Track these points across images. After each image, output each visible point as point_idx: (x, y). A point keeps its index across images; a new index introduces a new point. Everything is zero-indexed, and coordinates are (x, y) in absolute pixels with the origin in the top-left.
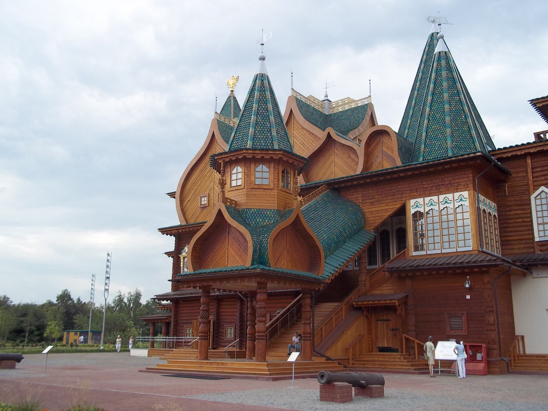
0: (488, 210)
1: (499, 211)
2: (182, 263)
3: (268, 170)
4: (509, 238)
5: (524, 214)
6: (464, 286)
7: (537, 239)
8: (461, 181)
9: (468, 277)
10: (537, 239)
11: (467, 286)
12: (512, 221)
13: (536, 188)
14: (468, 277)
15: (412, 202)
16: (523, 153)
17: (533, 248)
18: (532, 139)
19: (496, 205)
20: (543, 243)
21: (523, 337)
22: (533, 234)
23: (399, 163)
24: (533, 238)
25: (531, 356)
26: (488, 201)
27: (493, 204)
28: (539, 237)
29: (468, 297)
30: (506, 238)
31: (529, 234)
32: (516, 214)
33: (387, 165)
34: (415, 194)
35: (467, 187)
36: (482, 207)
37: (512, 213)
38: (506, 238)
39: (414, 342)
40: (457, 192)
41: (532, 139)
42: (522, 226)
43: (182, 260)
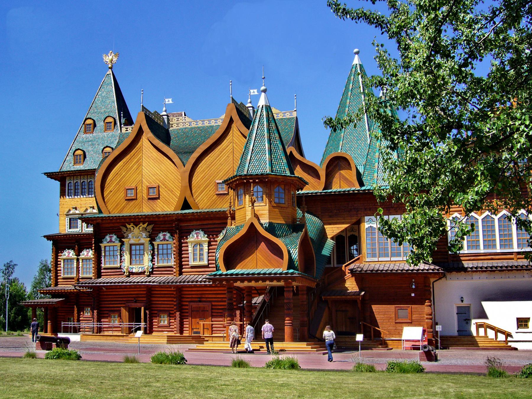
2: (103, 252)
9: (413, 280)
11: (414, 287)
15: (367, 218)
29: (413, 295)
34: (369, 212)
39: (370, 328)
43: (103, 249)
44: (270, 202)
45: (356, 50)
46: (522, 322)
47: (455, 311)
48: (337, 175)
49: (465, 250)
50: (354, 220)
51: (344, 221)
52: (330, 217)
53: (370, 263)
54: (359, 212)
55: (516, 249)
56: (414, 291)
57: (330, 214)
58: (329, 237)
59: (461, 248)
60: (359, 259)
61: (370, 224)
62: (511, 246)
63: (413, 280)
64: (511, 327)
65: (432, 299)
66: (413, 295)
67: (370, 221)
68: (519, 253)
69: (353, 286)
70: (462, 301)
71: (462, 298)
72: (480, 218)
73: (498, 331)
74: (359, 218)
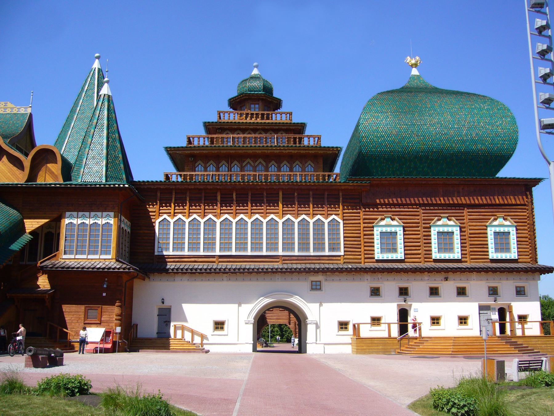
7: (156, 254)
9: (106, 279)
10: (156, 254)
11: (105, 286)
13: (160, 214)
14: (106, 279)
18: (163, 179)
21: (137, 325)
23: (61, 182)
24: (154, 252)
25: (140, 339)
27: (129, 223)
29: (104, 294)
33: (50, 180)
37: (141, 232)
41: (163, 179)
45: (97, 55)
46: (219, 325)
47: (156, 312)
49: (171, 252)
53: (66, 260)
55: (218, 253)
56: (106, 290)
59: (167, 249)
60: (55, 255)
61: (71, 221)
62: (213, 249)
64: (208, 329)
65: (123, 299)
67: (71, 217)
68: (221, 257)
69: (45, 284)
70: (163, 303)
71: (163, 299)
73: (193, 332)
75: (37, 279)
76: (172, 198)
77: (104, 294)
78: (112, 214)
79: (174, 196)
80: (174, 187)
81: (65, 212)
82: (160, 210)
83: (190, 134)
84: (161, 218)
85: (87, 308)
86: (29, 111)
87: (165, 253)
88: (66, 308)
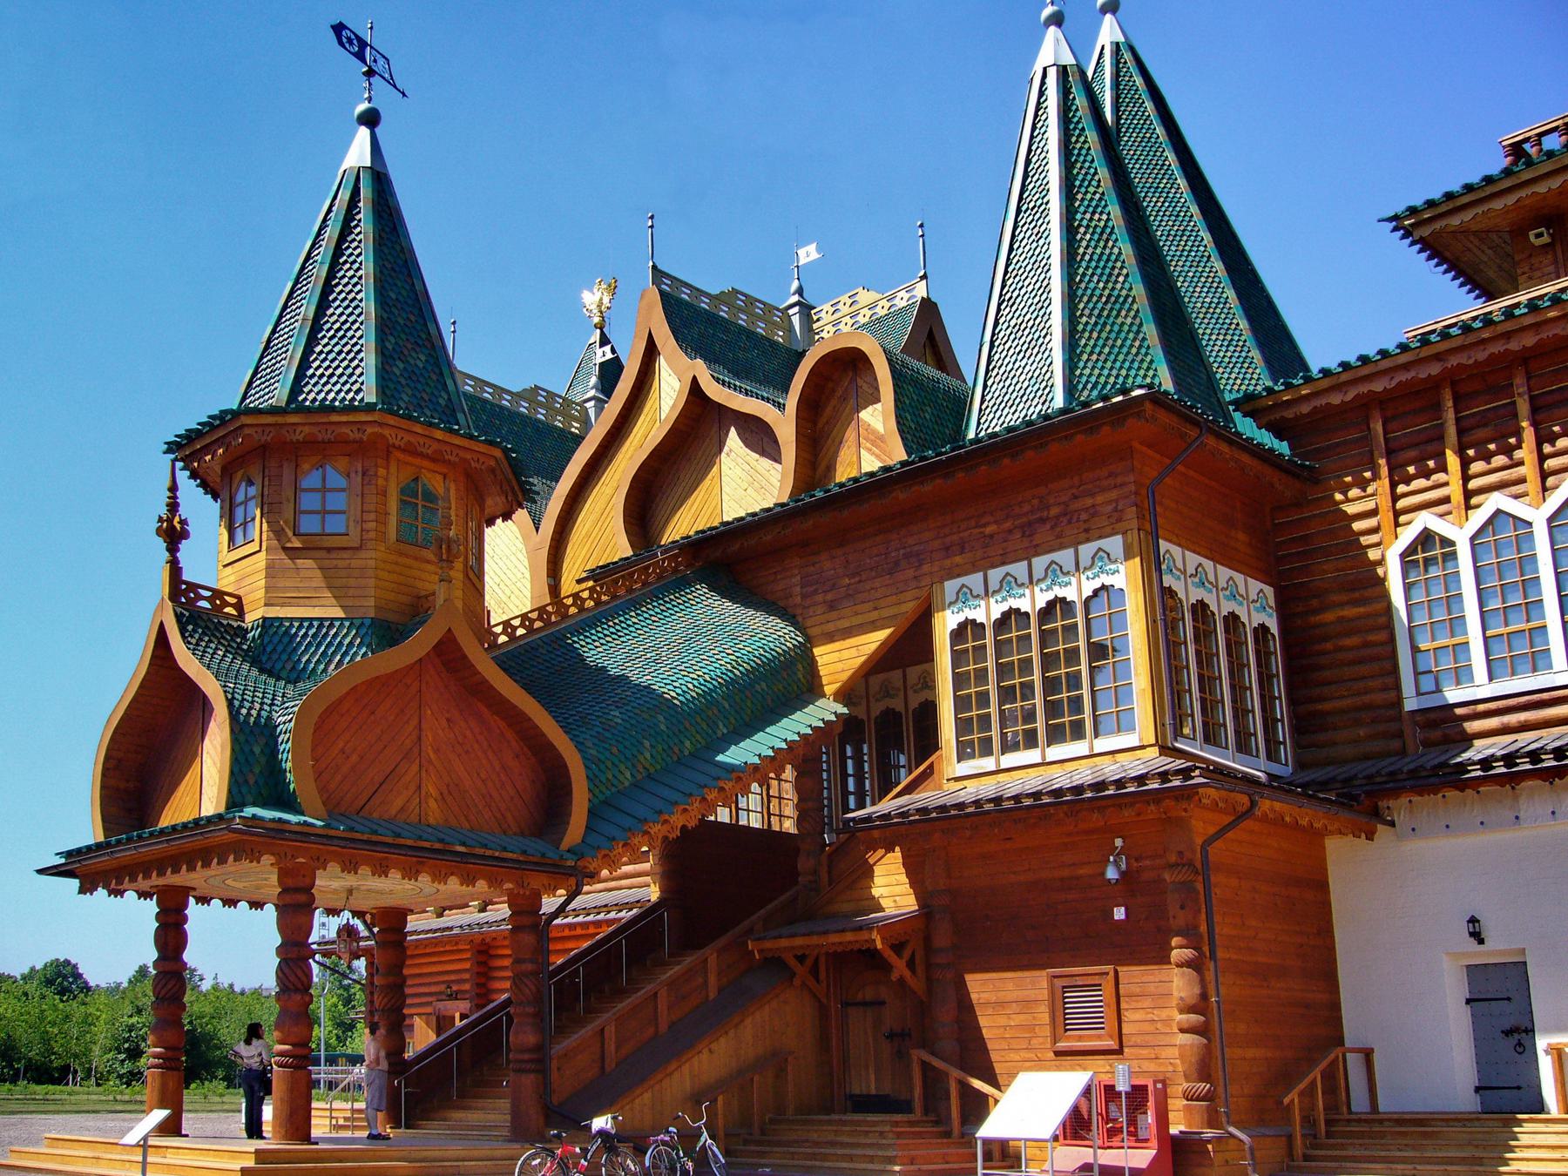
0: (1221, 607)
1: (1283, 608)
3: (343, 483)
4: (1327, 706)
5: (1368, 615)
6: (1103, 874)
7: (1410, 704)
8: (1099, 499)
10: (1410, 704)
11: (1111, 874)
12: (1329, 646)
16: (1350, 396)
17: (1399, 735)
19: (1269, 591)
20: (1432, 716)
22: (1397, 687)
26: (1224, 573)
27: (1255, 586)
28: (1419, 694)
30: (1311, 707)
31: (1385, 689)
32: (1341, 619)
35: (1119, 520)
36: (1190, 594)
37: (1329, 616)
38: (1311, 707)
40: (1088, 540)
42: (1360, 661)
44: (278, 533)
47: (1453, 991)
48: (850, 434)
49: (1481, 687)
50: (909, 607)
51: (875, 615)
52: (832, 606)
53: (965, 783)
54: (926, 568)
57: (829, 597)
58: (829, 690)
59: (1462, 675)
60: (931, 766)
63: (1118, 842)
65: (1203, 928)
66: (1119, 913)
69: (898, 890)
71: (1473, 920)
72: (1538, 515)
74: (924, 593)
75: (868, 872)
76: (1441, 427)
77: (1119, 913)
78: (1114, 544)
79: (1450, 415)
80: (1435, 369)
81: (942, 581)
82: (1395, 498)
83: (1517, 135)
84: (1407, 535)
85: (1059, 983)
86: (921, 291)
87: (1453, 695)
88: (982, 987)
